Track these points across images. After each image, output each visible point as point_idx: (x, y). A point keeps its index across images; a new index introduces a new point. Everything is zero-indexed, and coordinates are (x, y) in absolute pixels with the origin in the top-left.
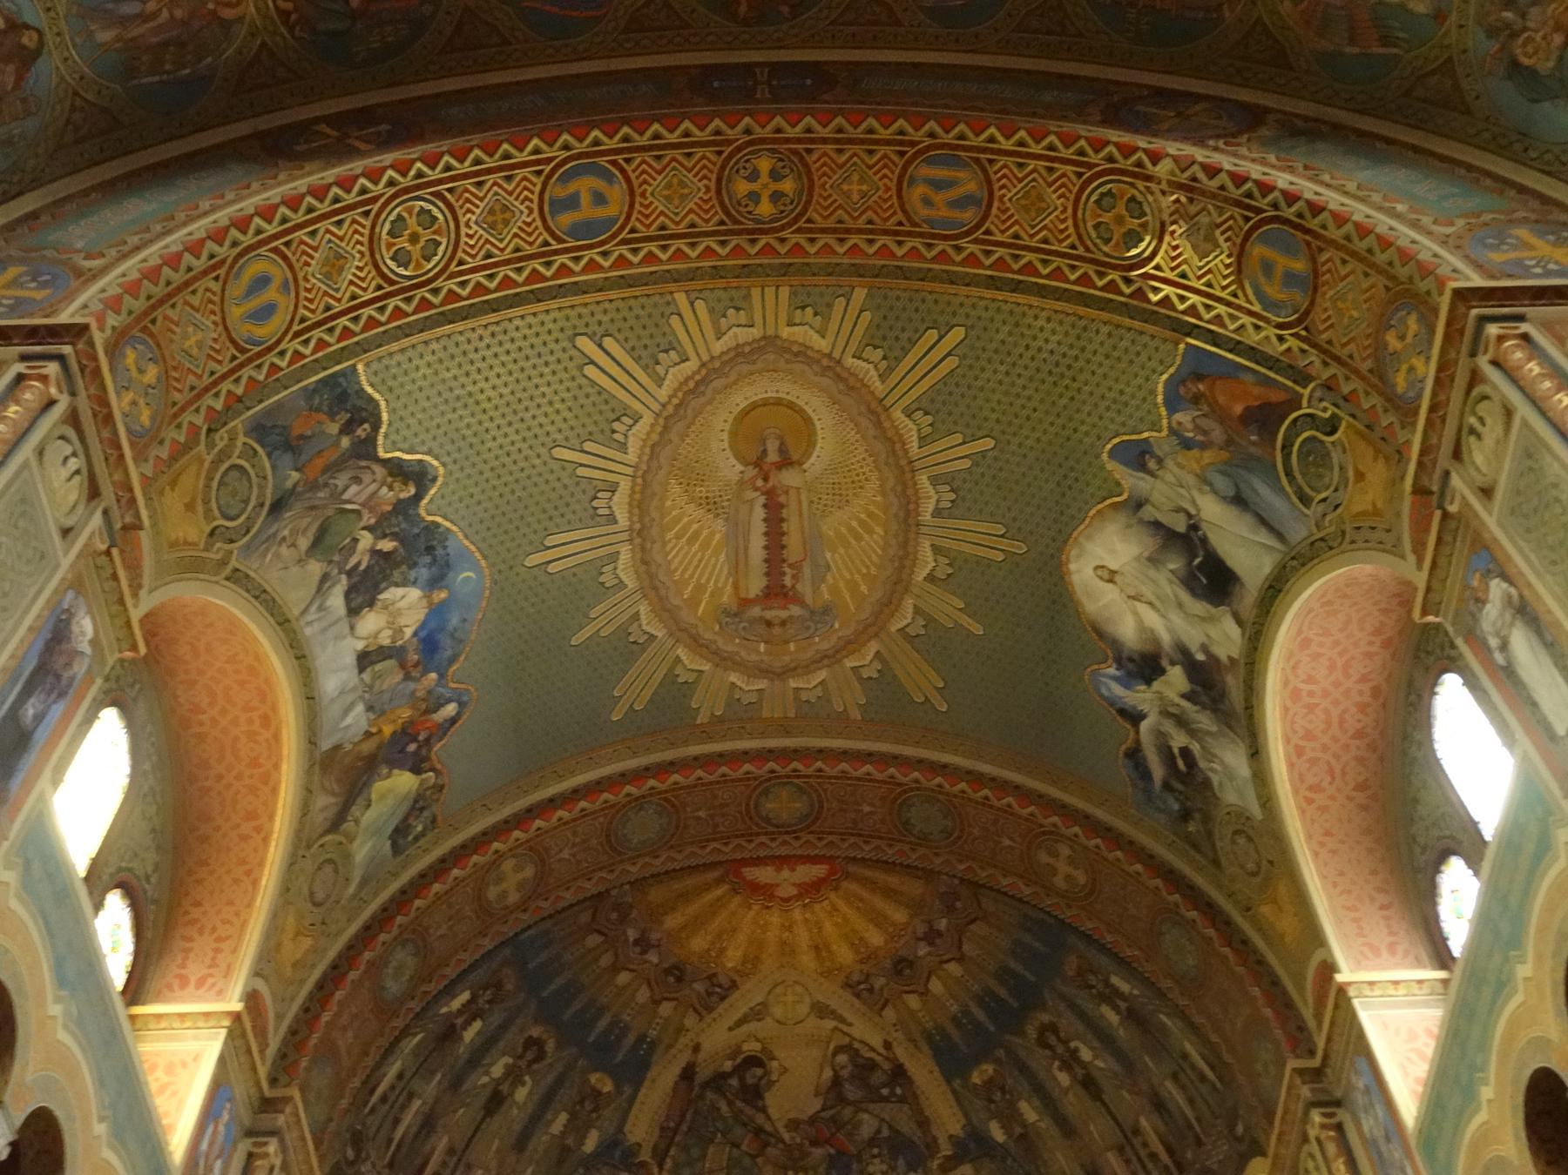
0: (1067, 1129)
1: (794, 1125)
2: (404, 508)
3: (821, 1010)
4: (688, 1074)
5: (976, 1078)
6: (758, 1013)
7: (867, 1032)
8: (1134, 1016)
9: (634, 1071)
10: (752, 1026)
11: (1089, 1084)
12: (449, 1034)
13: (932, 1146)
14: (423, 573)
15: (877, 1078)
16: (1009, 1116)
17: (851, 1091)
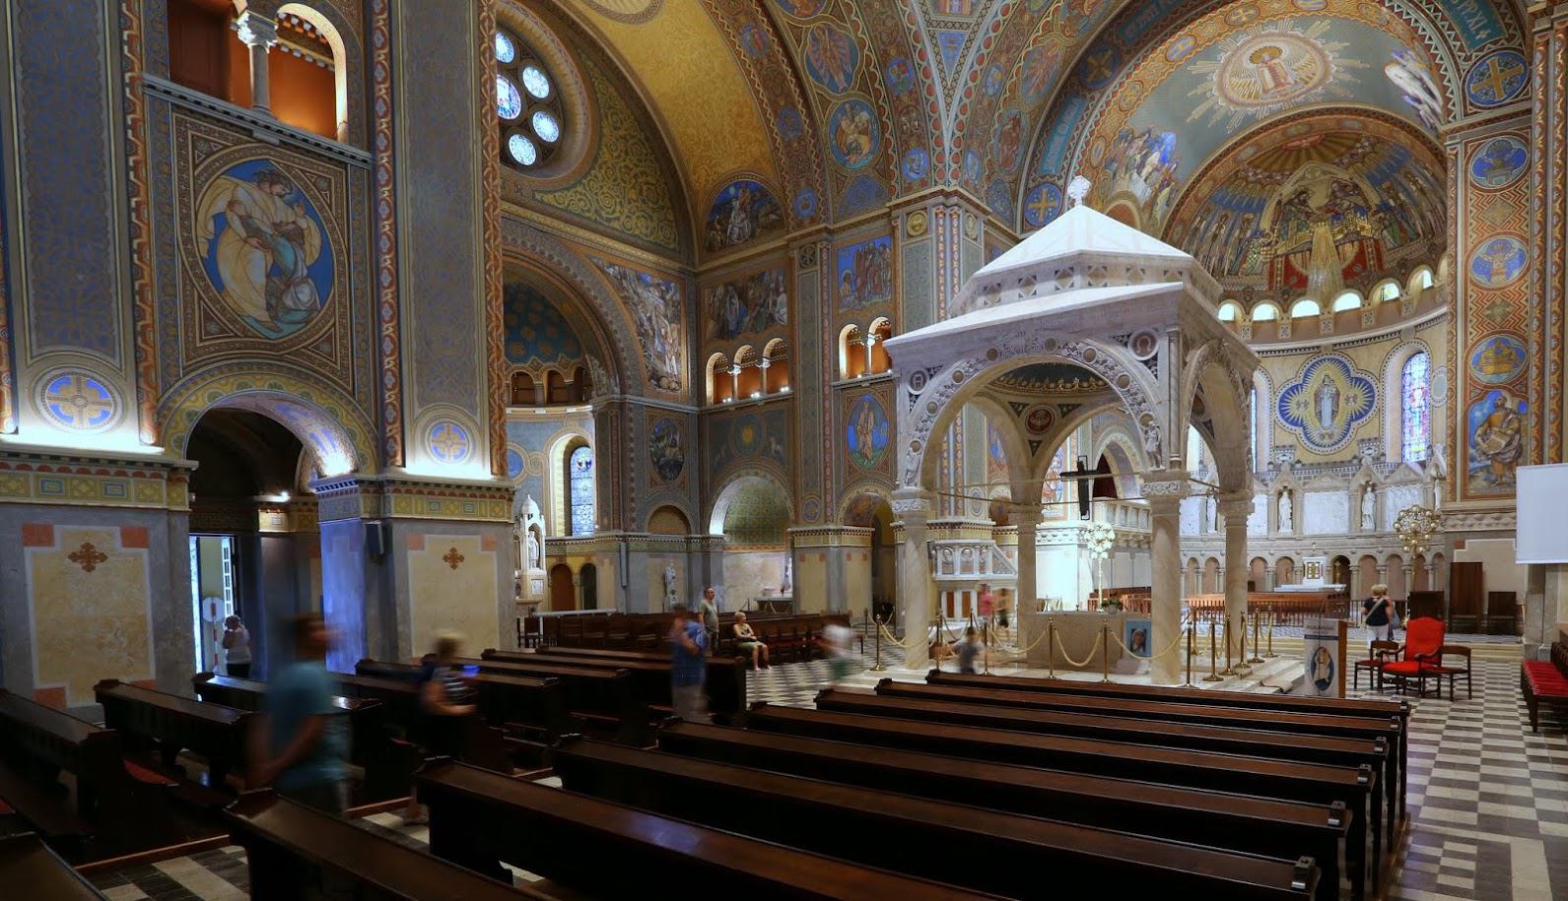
0: (1416, 204)
1: (1319, 208)
2: (1145, 142)
3: (1324, 173)
4: (1279, 202)
5: (1384, 186)
6: (1302, 178)
7: (1344, 176)
8: (1433, 175)
9: (1260, 208)
10: (1300, 183)
11: (1421, 190)
12: (1197, 229)
13: (1370, 208)
14: (1156, 148)
15: (1348, 189)
16: (1396, 198)
17: (1339, 195)
